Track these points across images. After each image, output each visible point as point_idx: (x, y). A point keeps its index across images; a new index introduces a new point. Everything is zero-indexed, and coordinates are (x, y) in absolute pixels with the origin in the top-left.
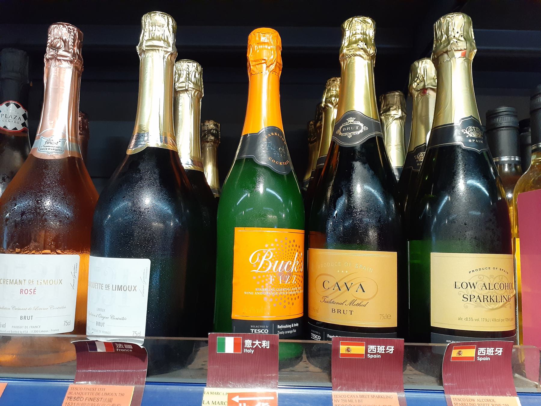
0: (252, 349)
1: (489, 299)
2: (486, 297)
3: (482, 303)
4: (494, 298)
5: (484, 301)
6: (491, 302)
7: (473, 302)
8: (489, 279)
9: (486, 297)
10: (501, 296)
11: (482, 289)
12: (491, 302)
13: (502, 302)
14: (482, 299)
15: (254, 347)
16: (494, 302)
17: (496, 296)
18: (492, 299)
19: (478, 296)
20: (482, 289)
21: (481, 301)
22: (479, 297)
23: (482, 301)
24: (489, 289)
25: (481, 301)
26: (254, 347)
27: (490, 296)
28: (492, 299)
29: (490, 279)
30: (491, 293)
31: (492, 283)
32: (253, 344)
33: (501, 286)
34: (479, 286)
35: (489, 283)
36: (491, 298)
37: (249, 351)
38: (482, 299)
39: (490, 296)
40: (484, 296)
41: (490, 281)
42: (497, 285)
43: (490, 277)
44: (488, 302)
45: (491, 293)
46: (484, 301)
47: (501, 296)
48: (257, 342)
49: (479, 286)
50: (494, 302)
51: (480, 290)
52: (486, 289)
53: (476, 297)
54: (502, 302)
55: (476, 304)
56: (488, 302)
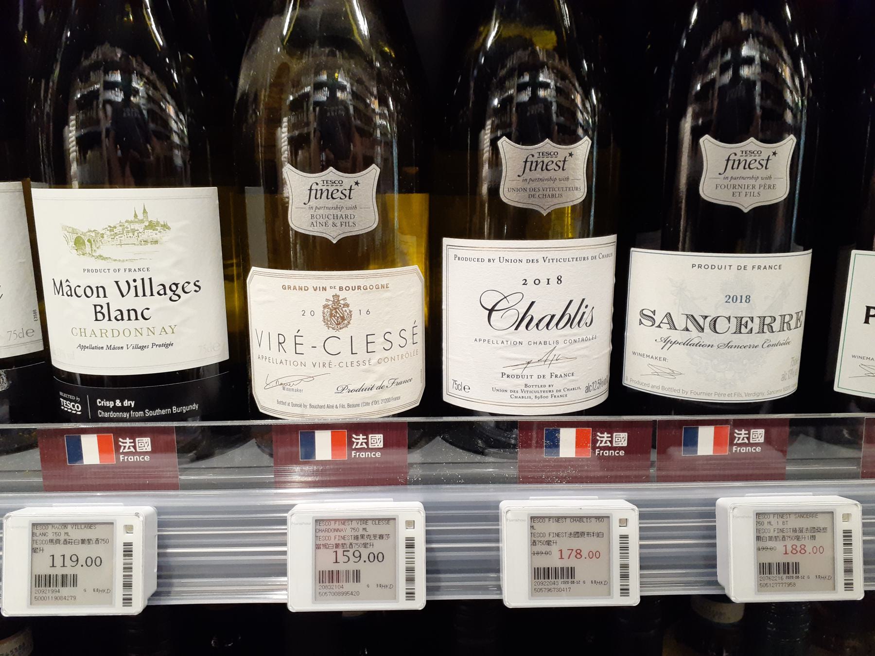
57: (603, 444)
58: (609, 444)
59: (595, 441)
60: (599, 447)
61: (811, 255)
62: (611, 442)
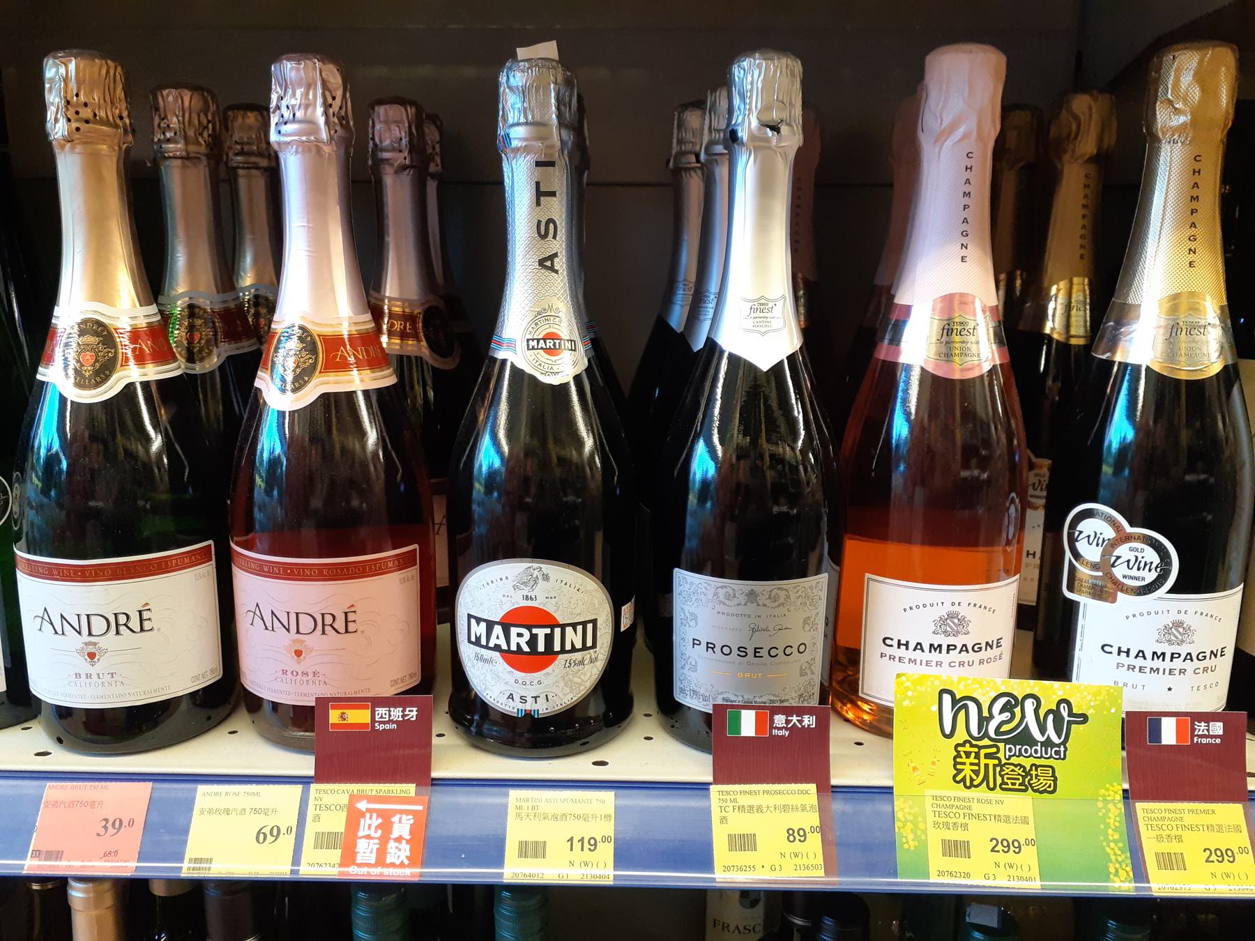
0: (786, 729)
15: (789, 726)
26: (789, 726)
32: (788, 722)
37: (781, 733)
48: (795, 719)
57: (1200, 733)
58: (1206, 732)
59: (1193, 730)
60: (1197, 735)
61: (1016, 584)
62: (1208, 730)
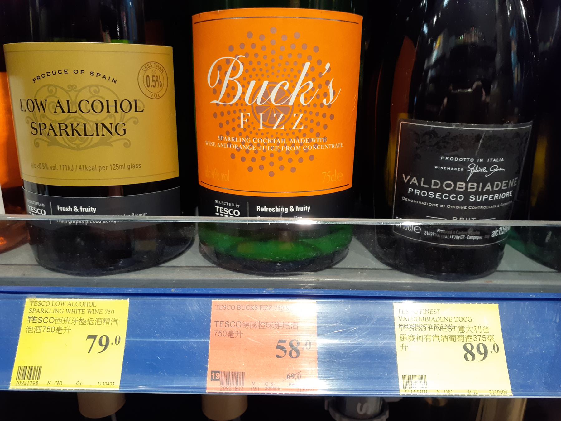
1: (69, 130)
2: (63, 127)
3: (58, 138)
4: (81, 129)
5: (61, 135)
6: (73, 135)
7: (45, 135)
8: (68, 94)
9: (63, 127)
10: (97, 125)
11: (55, 112)
12: (73, 135)
13: (98, 135)
14: (57, 130)
16: (79, 135)
17: (85, 125)
18: (76, 131)
19: (51, 125)
20: (55, 112)
21: (56, 135)
22: (52, 127)
23: (58, 134)
24: (69, 112)
25: (56, 135)
27: (72, 125)
28: (76, 131)
29: (69, 92)
30: (73, 119)
31: (73, 99)
33: (97, 106)
34: (51, 106)
35: (68, 101)
36: (74, 128)
38: (57, 130)
39: (72, 125)
40: (59, 124)
41: (70, 96)
42: (86, 105)
43: (69, 88)
44: (68, 135)
45: (73, 119)
46: (61, 135)
47: (97, 125)
49: (51, 106)
50: (79, 135)
51: (51, 113)
52: (63, 112)
53: (48, 125)
54: (98, 135)
55: (48, 138)
56: (68, 135)
